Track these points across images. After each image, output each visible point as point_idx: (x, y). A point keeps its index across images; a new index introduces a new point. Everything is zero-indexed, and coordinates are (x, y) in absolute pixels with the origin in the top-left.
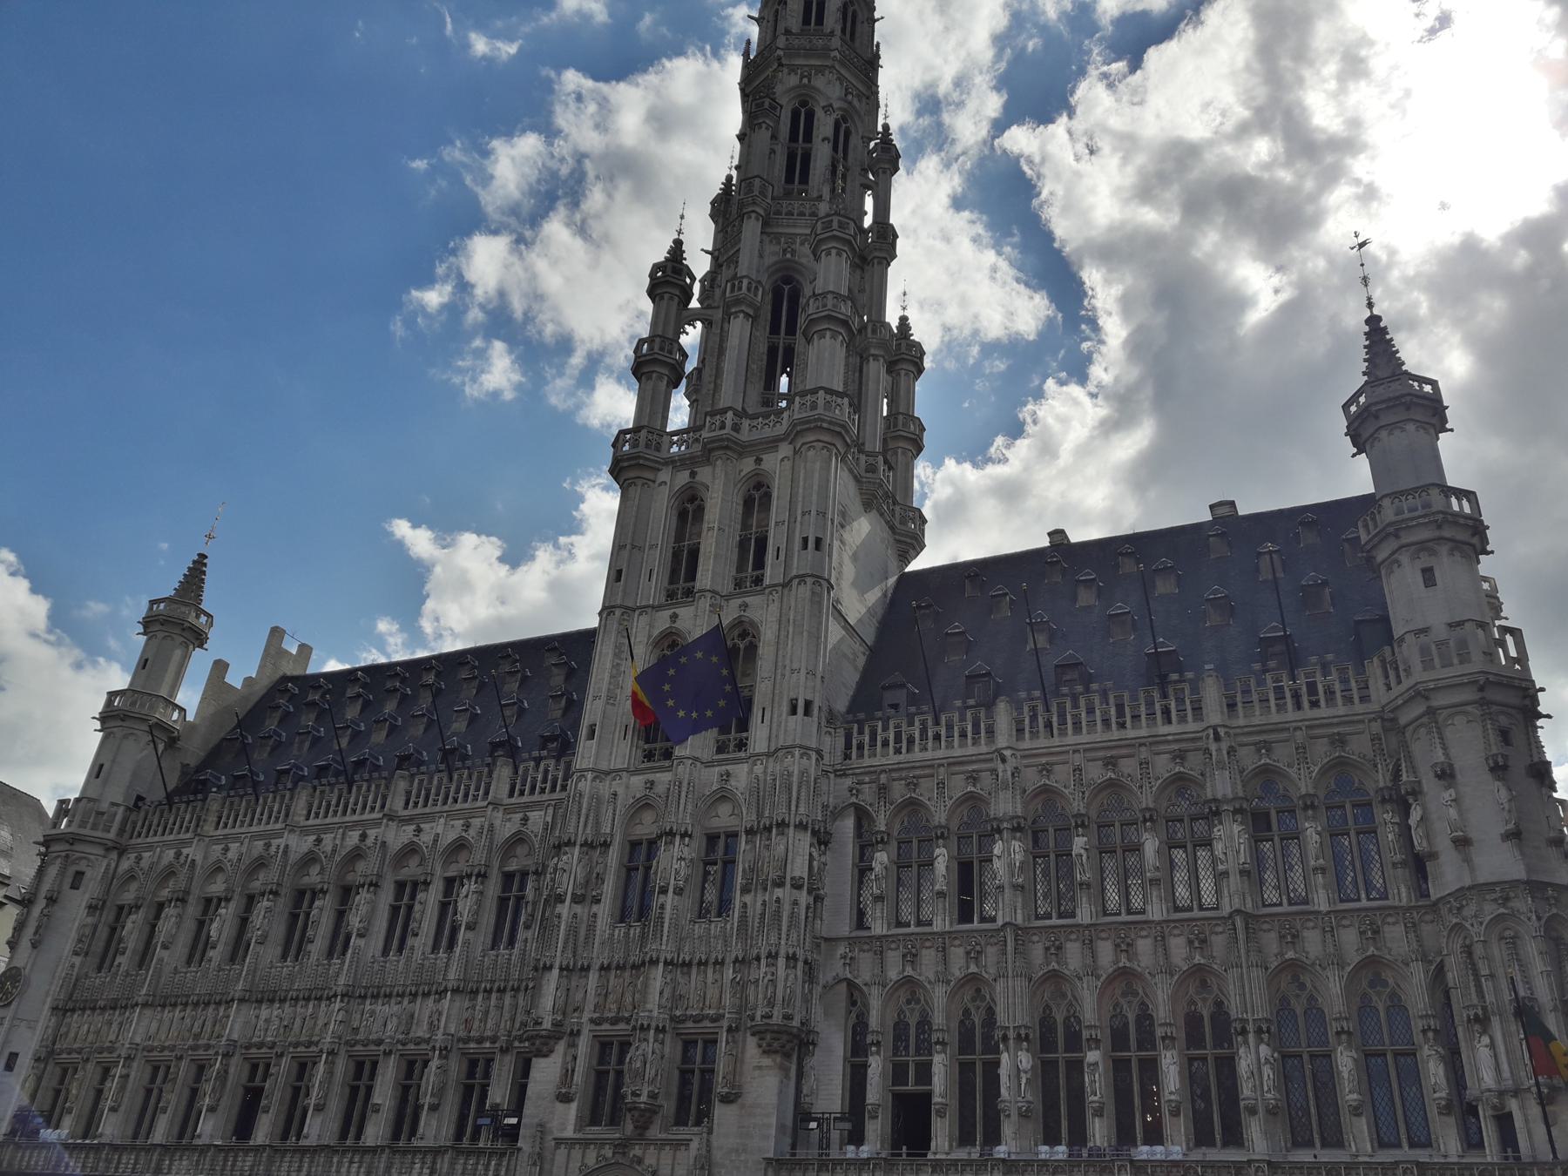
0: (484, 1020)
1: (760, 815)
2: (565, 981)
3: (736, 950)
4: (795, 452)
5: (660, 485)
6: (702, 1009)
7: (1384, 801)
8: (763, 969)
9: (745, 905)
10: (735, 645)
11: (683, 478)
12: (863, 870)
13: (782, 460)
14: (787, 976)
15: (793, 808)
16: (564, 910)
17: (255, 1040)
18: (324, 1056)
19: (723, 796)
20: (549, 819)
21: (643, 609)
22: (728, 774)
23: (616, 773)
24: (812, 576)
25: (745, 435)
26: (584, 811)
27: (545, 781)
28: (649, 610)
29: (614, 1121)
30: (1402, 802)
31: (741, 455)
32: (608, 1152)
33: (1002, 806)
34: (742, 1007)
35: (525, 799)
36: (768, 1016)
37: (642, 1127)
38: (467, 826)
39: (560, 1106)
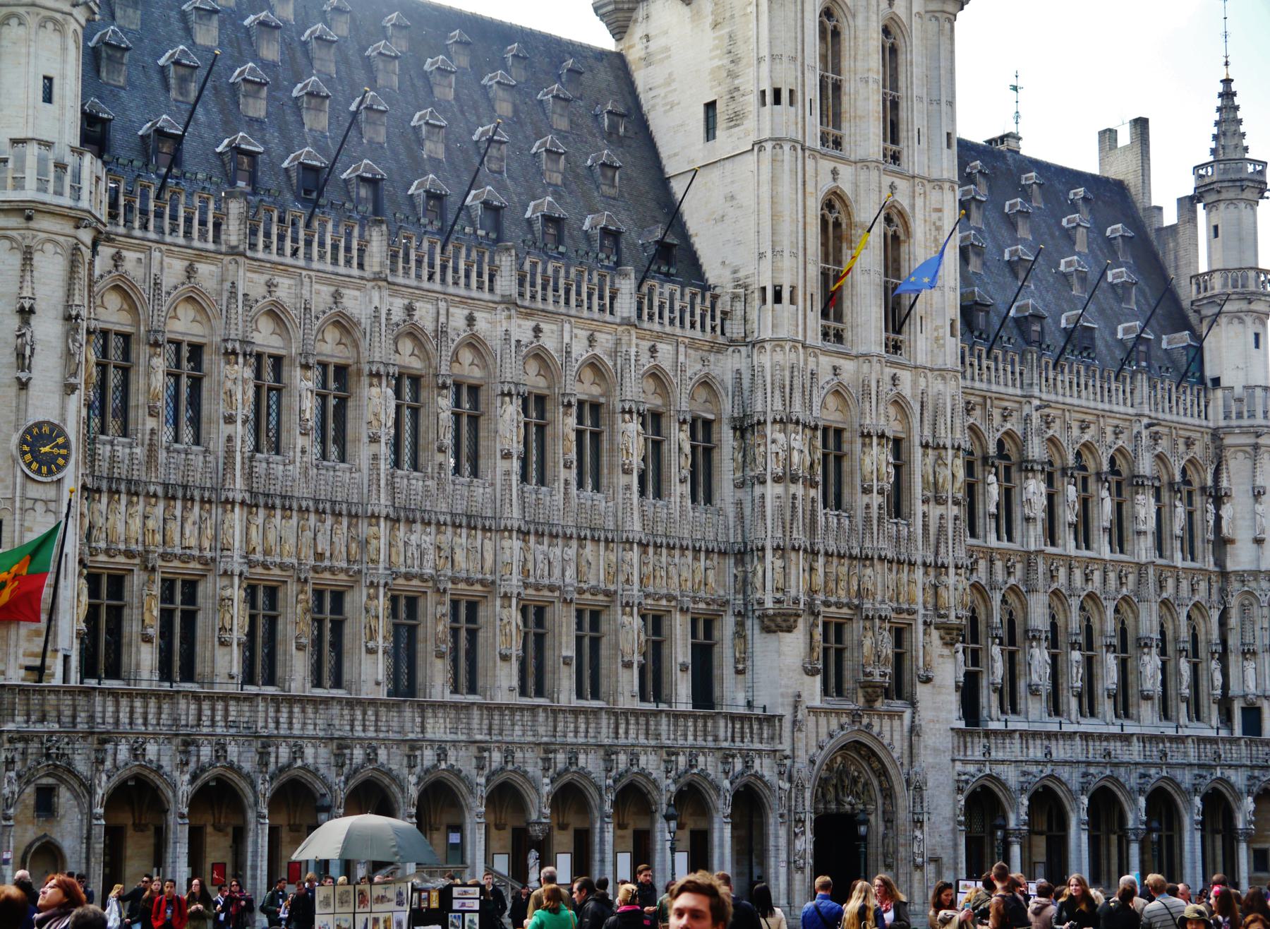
4: (927, 12)
7: (1210, 495)
9: (924, 515)
16: (798, 489)
17: (403, 570)
18: (514, 601)
19: (899, 403)
27: (672, 311)
28: (818, 156)
30: (1218, 498)
32: (845, 719)
33: (1037, 450)
35: (656, 327)
37: (870, 701)
38: (591, 340)
39: (806, 677)
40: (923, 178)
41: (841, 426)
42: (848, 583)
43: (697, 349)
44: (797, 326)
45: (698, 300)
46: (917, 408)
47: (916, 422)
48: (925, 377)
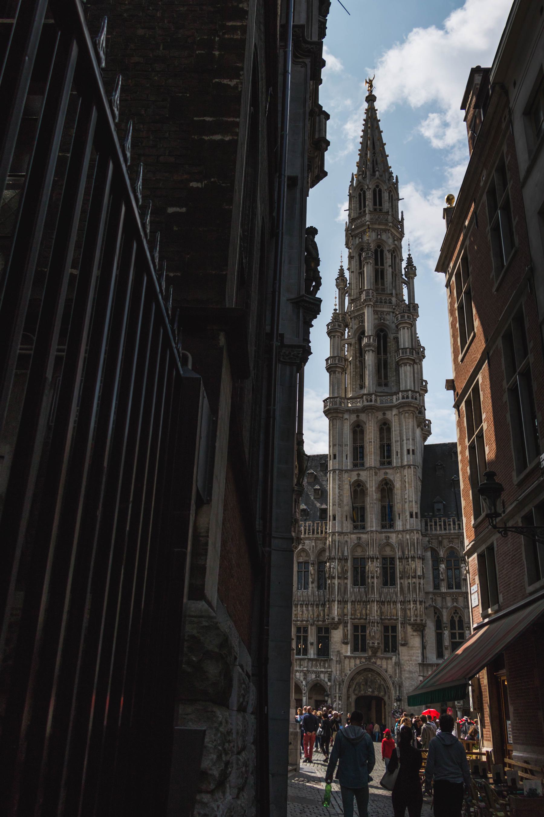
0: (302, 614)
1: (403, 553)
2: (340, 606)
3: (400, 598)
4: (399, 413)
5: (345, 419)
6: (391, 616)
8: (412, 605)
9: (401, 583)
10: (383, 487)
11: (354, 417)
12: (436, 569)
13: (394, 415)
14: (420, 608)
15: (416, 552)
16: (336, 581)
19: (388, 544)
20: (313, 544)
21: (347, 471)
22: (389, 537)
23: (346, 534)
24: (413, 465)
25: (378, 404)
26: (337, 547)
27: (309, 530)
28: (349, 472)
29: (364, 650)
31: (377, 411)
32: (363, 660)
34: (405, 616)
36: (416, 620)
39: (343, 645)
40: (398, 467)
41: (362, 557)
42: (362, 610)
43: (321, 540)
44: (336, 527)
45: (320, 525)
46: (397, 545)
47: (397, 551)
48: (401, 534)
